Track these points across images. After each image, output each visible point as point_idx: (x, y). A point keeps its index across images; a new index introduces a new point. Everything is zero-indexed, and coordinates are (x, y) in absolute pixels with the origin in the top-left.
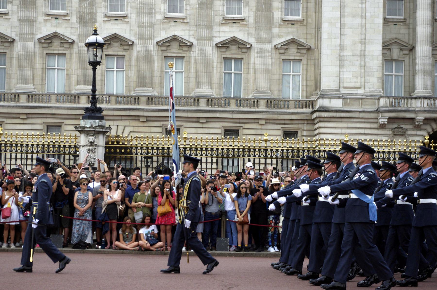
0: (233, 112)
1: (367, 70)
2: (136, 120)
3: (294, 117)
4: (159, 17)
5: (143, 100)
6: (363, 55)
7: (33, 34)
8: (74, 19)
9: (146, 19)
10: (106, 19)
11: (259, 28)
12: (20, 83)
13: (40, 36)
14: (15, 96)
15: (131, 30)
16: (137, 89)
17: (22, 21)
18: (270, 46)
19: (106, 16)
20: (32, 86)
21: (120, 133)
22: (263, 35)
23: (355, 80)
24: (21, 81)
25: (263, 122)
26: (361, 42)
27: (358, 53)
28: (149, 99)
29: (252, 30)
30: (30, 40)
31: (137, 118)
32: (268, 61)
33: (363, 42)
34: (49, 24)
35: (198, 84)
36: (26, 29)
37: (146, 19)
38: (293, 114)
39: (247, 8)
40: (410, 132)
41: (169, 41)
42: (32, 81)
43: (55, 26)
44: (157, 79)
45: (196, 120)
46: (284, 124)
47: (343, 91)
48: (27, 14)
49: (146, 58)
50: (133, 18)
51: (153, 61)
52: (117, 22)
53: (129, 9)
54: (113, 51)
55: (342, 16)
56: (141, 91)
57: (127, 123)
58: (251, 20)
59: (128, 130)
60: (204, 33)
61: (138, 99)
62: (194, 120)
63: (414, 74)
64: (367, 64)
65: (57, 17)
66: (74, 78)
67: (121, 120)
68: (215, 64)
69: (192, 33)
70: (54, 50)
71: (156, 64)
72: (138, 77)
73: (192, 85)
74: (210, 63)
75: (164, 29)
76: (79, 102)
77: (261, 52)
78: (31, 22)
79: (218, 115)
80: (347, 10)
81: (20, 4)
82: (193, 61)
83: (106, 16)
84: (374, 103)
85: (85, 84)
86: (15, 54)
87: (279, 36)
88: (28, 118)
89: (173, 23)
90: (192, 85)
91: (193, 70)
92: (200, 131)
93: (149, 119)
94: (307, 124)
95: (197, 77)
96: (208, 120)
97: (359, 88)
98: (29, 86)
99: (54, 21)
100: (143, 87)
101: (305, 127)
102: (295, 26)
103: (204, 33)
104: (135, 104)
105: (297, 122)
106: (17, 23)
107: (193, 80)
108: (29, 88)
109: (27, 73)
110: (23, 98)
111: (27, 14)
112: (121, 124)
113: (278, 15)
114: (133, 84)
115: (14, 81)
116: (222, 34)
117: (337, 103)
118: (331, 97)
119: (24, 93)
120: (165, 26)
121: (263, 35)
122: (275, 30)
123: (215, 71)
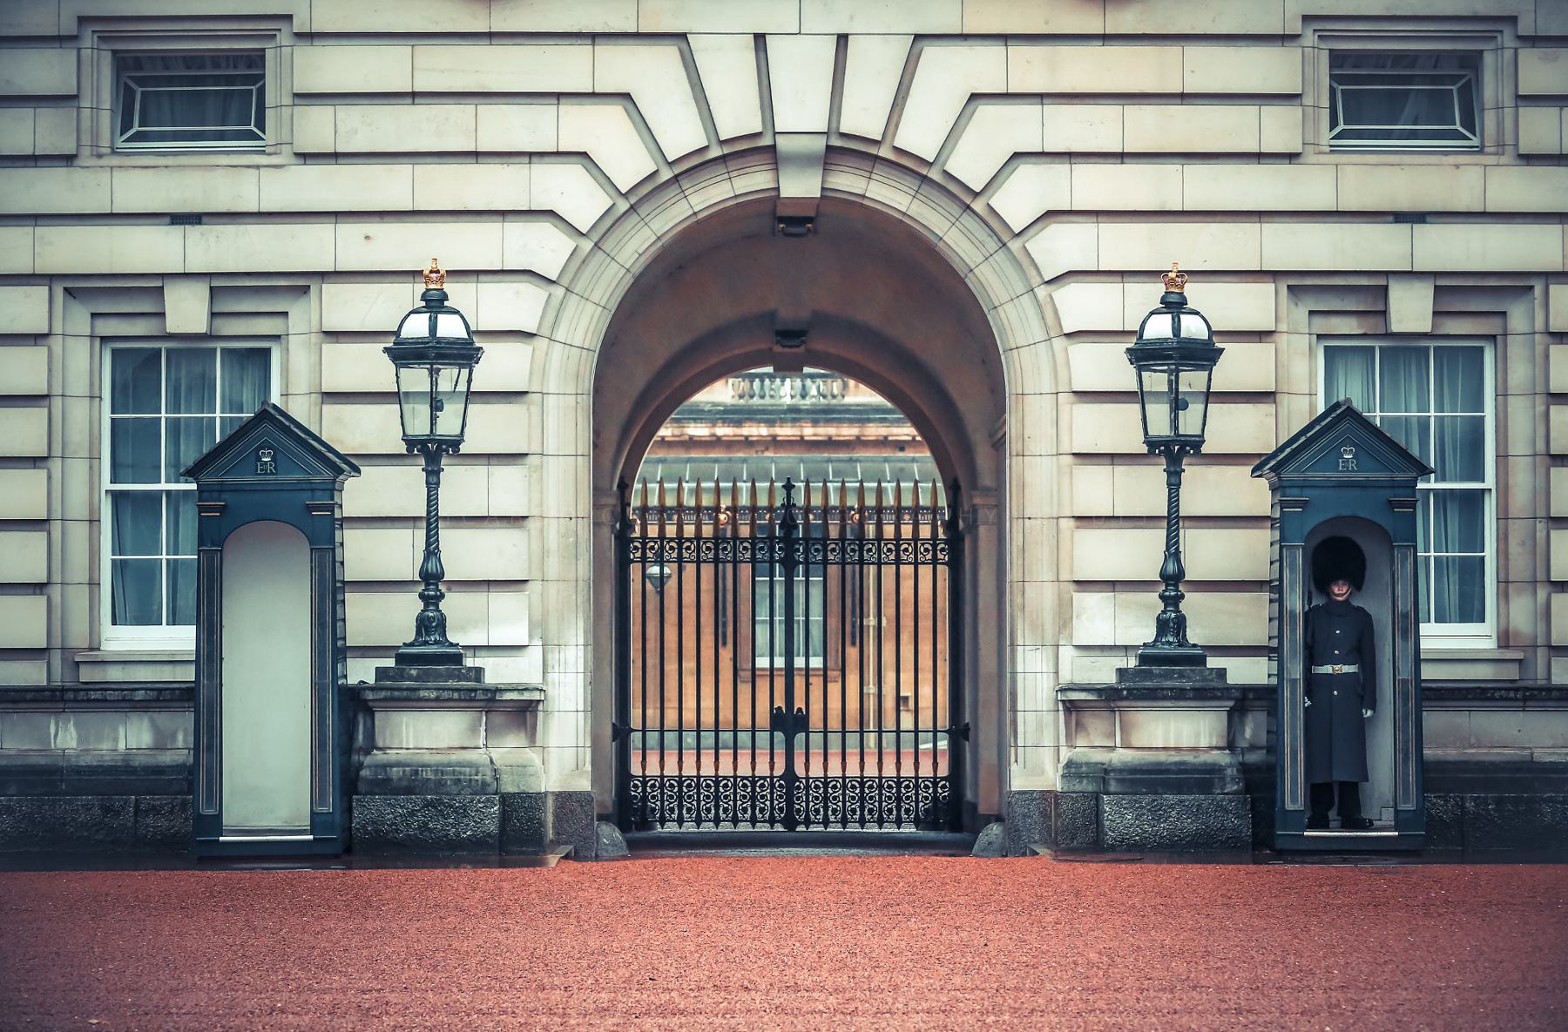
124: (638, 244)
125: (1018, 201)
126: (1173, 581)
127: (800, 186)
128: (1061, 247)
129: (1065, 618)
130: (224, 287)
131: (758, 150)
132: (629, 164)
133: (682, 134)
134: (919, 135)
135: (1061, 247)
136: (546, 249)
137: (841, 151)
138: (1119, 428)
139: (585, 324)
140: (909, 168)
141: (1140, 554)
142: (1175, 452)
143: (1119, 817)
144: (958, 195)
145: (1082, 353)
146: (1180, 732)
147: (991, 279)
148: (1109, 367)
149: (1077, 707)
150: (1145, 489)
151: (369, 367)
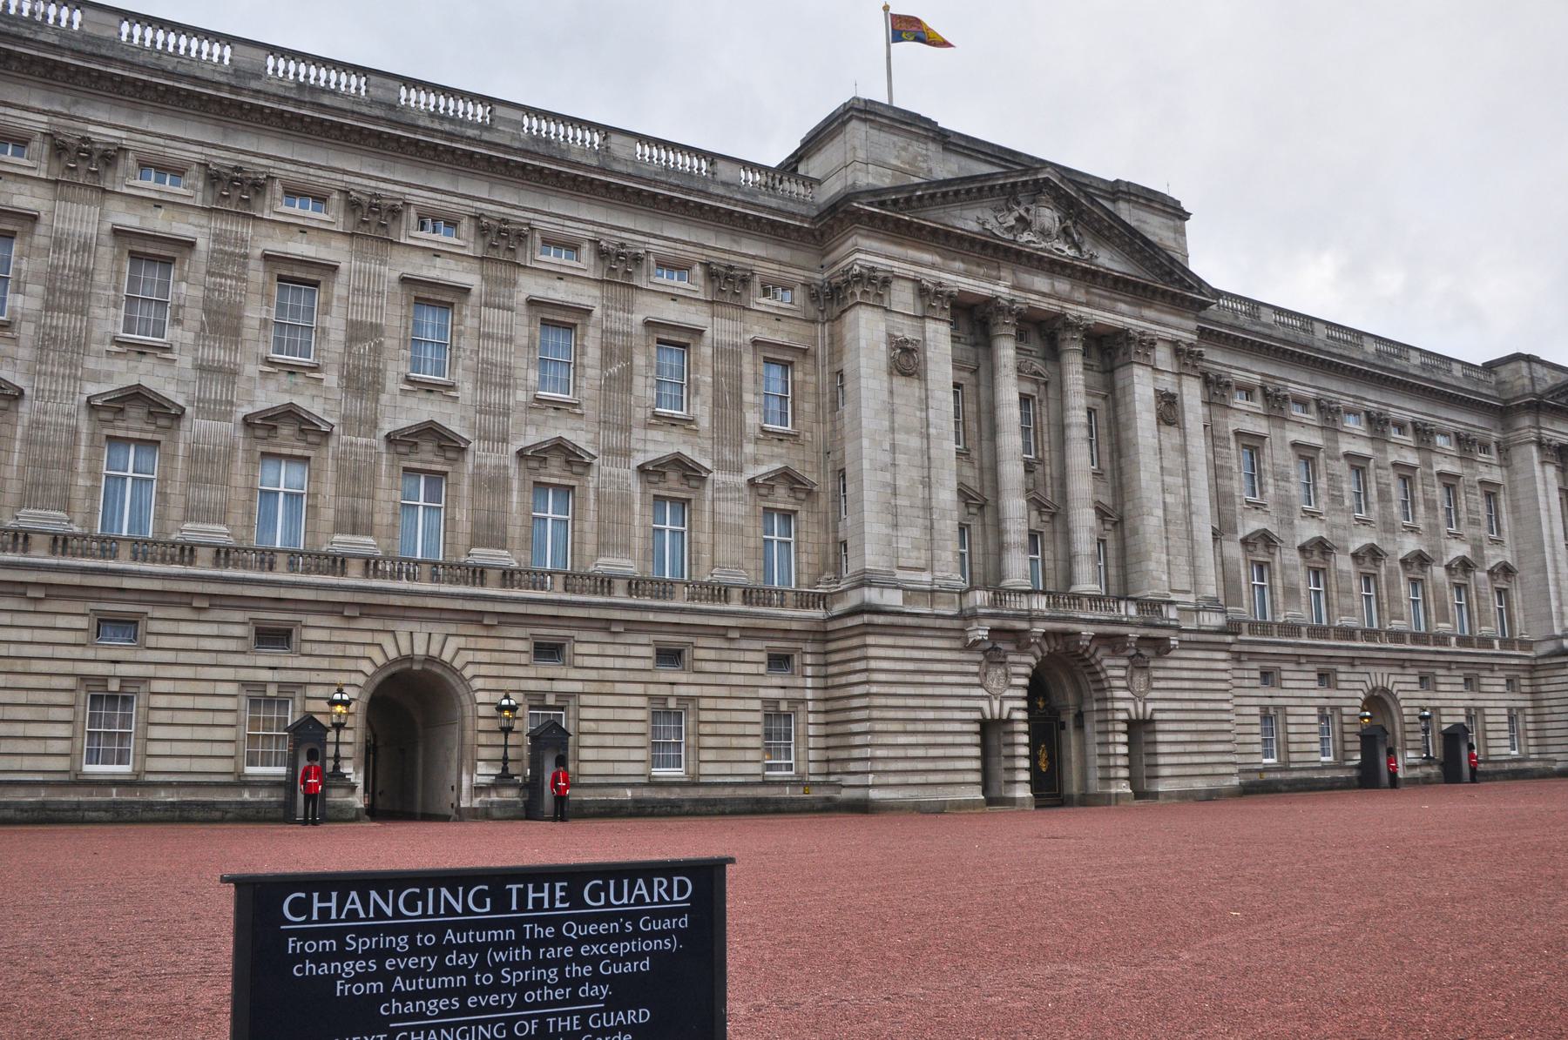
0: (682, 611)
1: (936, 536)
2: (471, 622)
3: (795, 626)
4: (521, 396)
5: (493, 575)
6: (928, 508)
7: (232, 403)
8: (331, 379)
9: (495, 397)
10: (408, 387)
11: (718, 441)
12: (192, 520)
13: (247, 410)
14: (183, 549)
15: (463, 418)
16: (473, 550)
17: (203, 368)
18: (742, 480)
19: (408, 380)
20: (223, 528)
21: (434, 651)
22: (728, 455)
23: (915, 554)
24: (192, 512)
25: (736, 634)
26: (922, 483)
27: (919, 503)
28: (504, 574)
29: (708, 444)
30: (226, 416)
31: (475, 618)
32: (740, 509)
33: (927, 483)
34: (271, 385)
35: (602, 547)
36: (216, 390)
37: (495, 397)
38: (792, 619)
39: (698, 399)
40: (1011, 658)
41: (545, 451)
42: (221, 516)
43: (286, 391)
44: (515, 531)
45: (603, 625)
46: (773, 639)
47: (900, 575)
48: (217, 353)
49: (495, 484)
50: (466, 390)
51: (507, 490)
52: (432, 397)
53: (459, 371)
54: (422, 461)
55: (892, 430)
56: (481, 555)
57: (452, 629)
58: (705, 423)
59: (453, 643)
60: (616, 439)
61: (482, 572)
62: (598, 625)
63: (1001, 548)
64: (936, 525)
65: (292, 370)
66: (328, 514)
67: (440, 620)
68: (637, 507)
69: (590, 436)
70: (281, 445)
71: (515, 497)
72: (475, 524)
73: (590, 548)
74: (626, 504)
75: (533, 423)
76: (343, 574)
77: (725, 490)
78: (230, 374)
79: (651, 617)
80: (899, 419)
81: (203, 329)
82: (592, 496)
83: (408, 380)
84: (953, 602)
85: (354, 533)
86: (181, 446)
87: (757, 462)
88: (212, 606)
89: (551, 413)
90: (590, 548)
91: (591, 516)
92: (610, 650)
93: (506, 619)
94: (814, 641)
95: (601, 531)
96: (631, 626)
97: (923, 570)
98: (217, 527)
99: (284, 379)
100: (487, 546)
101: (809, 647)
102: (785, 444)
103: (616, 439)
104: (474, 584)
105: (796, 636)
106: (191, 375)
107: (591, 539)
108: (219, 533)
109: (211, 495)
110: (204, 554)
111: (217, 353)
112: (438, 630)
113: (752, 419)
114: (463, 540)
115: (176, 513)
116: (650, 446)
117: (893, 599)
118: (883, 586)
119: (208, 545)
120: (535, 416)
121: (728, 455)
122: (749, 449)
123: (637, 522)
124: (379, 679)
125: (468, 673)
126: (505, 760)
127: (416, 667)
128: (478, 683)
129: (475, 767)
130: (281, 684)
131: (410, 658)
132: (380, 660)
133: (393, 654)
134: (446, 657)
135: (478, 683)
136: (361, 680)
137: (429, 659)
138: (494, 725)
139: (365, 698)
140: (443, 664)
141: (499, 753)
142: (507, 731)
143: (496, 813)
144: (454, 671)
145: (481, 708)
146: (510, 795)
147: (461, 689)
148: (491, 711)
149: (478, 789)
150: (500, 739)
151: (324, 706)
